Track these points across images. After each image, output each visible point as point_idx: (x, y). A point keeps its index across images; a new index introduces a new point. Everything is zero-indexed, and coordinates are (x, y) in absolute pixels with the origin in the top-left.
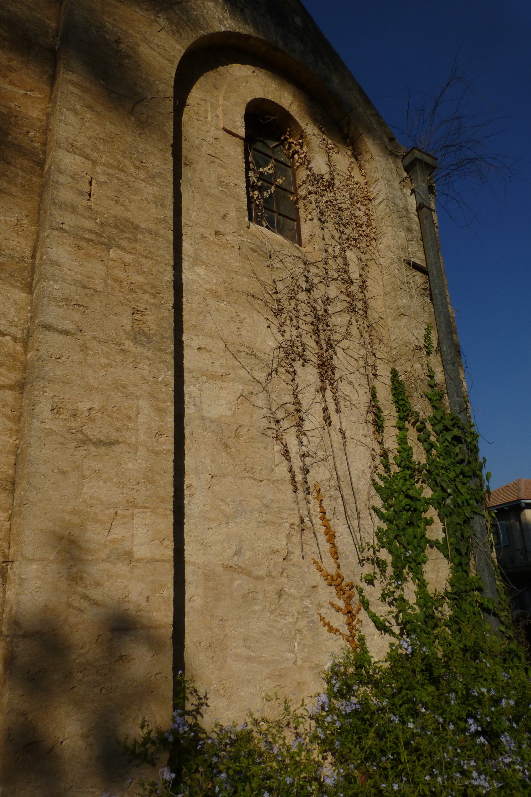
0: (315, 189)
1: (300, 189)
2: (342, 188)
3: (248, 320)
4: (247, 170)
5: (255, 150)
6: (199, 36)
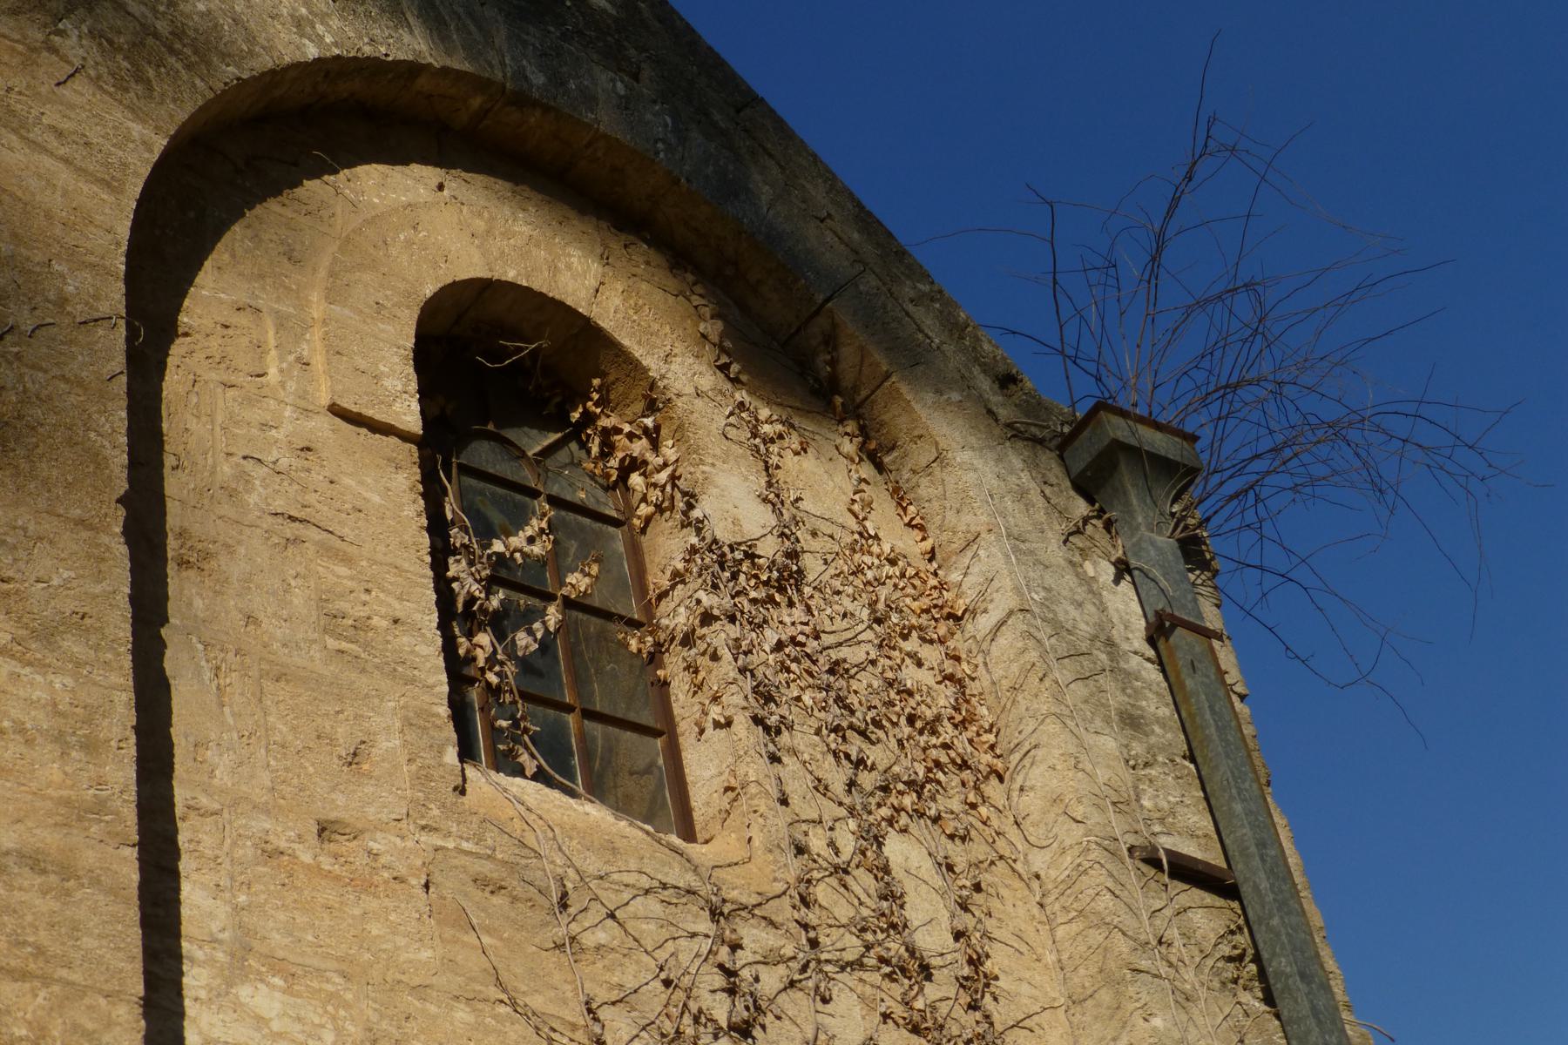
0: (727, 603)
1: (665, 606)
2: (837, 583)
4: (440, 554)
5: (465, 470)
6: (219, 86)
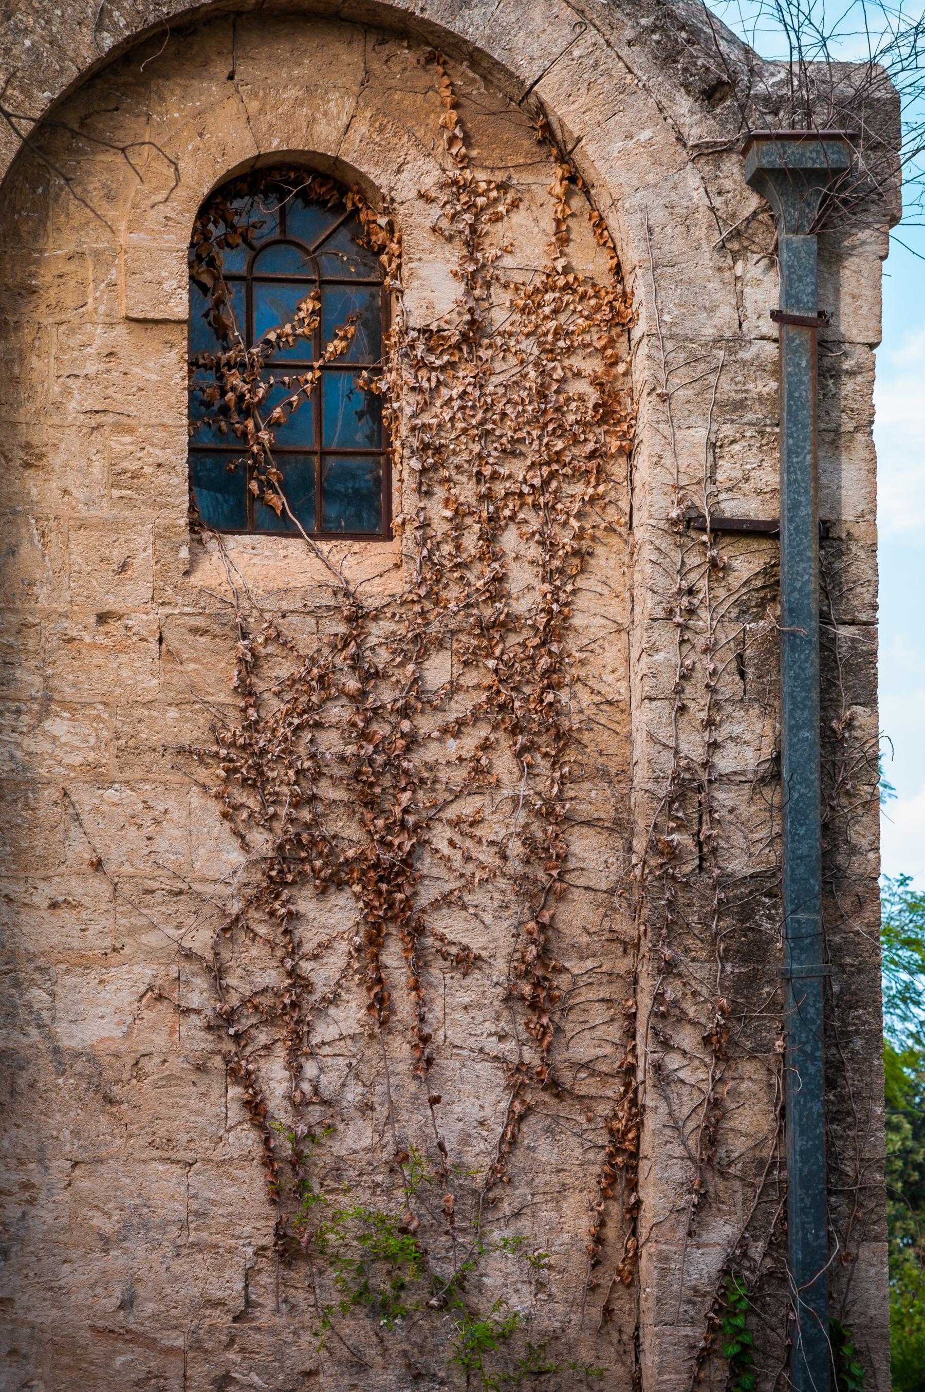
3: (174, 815)
